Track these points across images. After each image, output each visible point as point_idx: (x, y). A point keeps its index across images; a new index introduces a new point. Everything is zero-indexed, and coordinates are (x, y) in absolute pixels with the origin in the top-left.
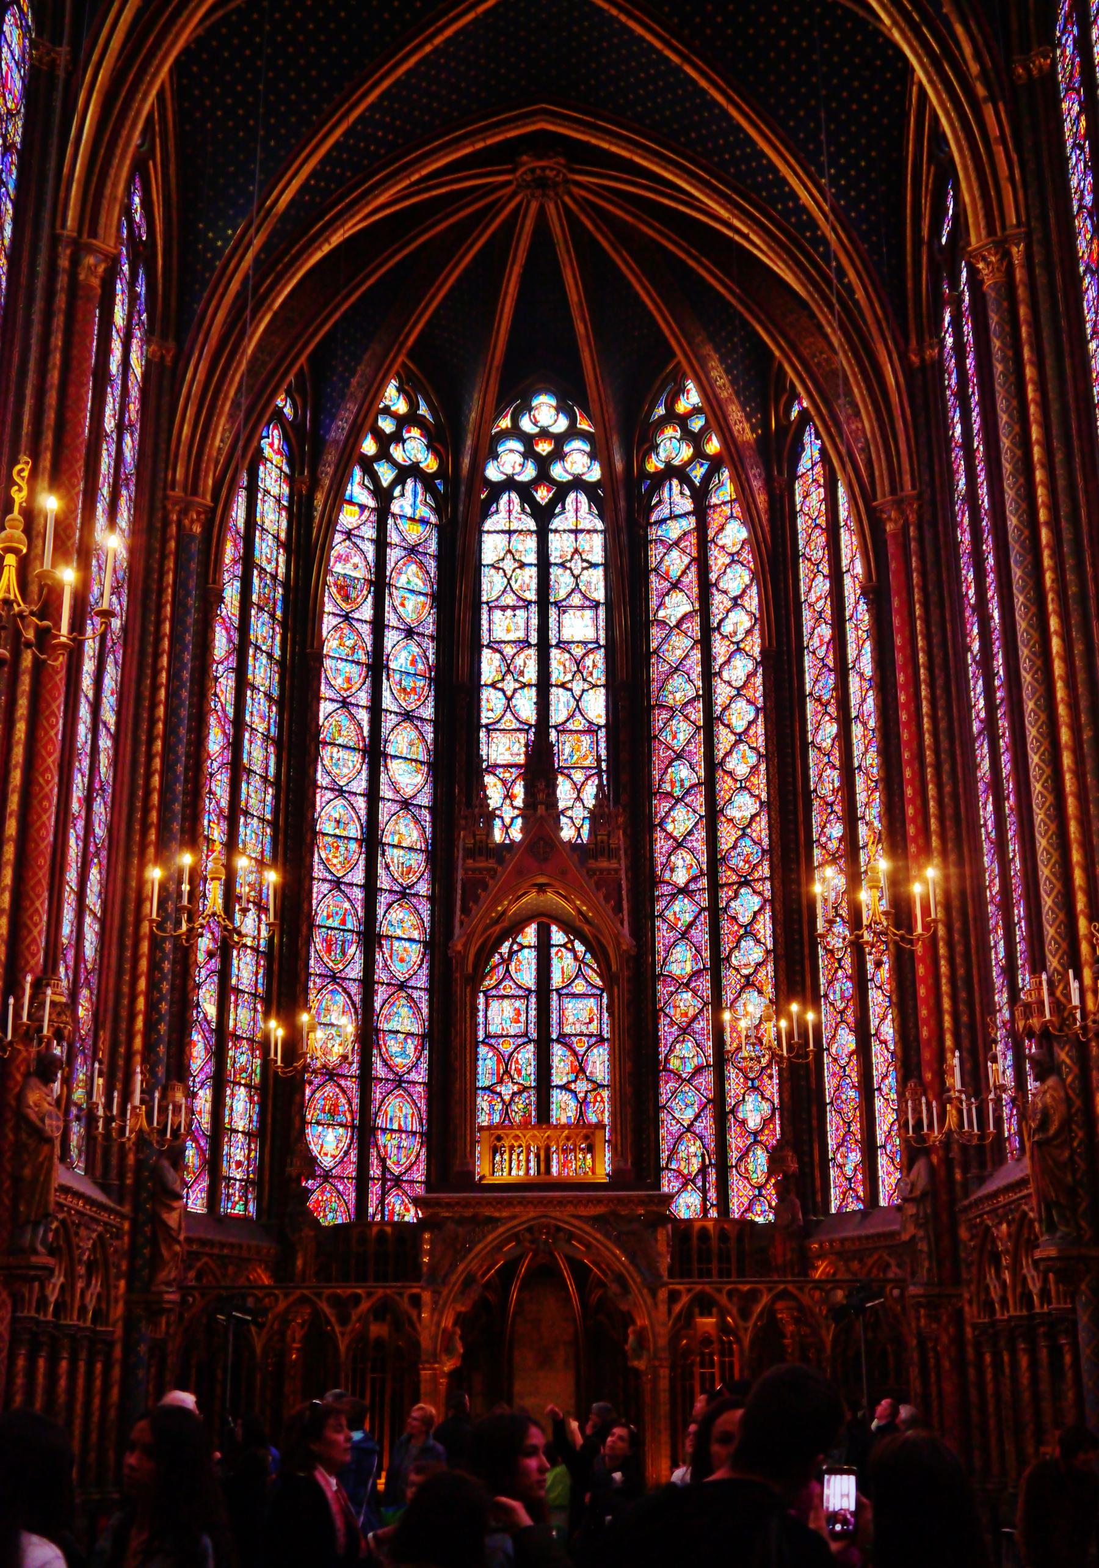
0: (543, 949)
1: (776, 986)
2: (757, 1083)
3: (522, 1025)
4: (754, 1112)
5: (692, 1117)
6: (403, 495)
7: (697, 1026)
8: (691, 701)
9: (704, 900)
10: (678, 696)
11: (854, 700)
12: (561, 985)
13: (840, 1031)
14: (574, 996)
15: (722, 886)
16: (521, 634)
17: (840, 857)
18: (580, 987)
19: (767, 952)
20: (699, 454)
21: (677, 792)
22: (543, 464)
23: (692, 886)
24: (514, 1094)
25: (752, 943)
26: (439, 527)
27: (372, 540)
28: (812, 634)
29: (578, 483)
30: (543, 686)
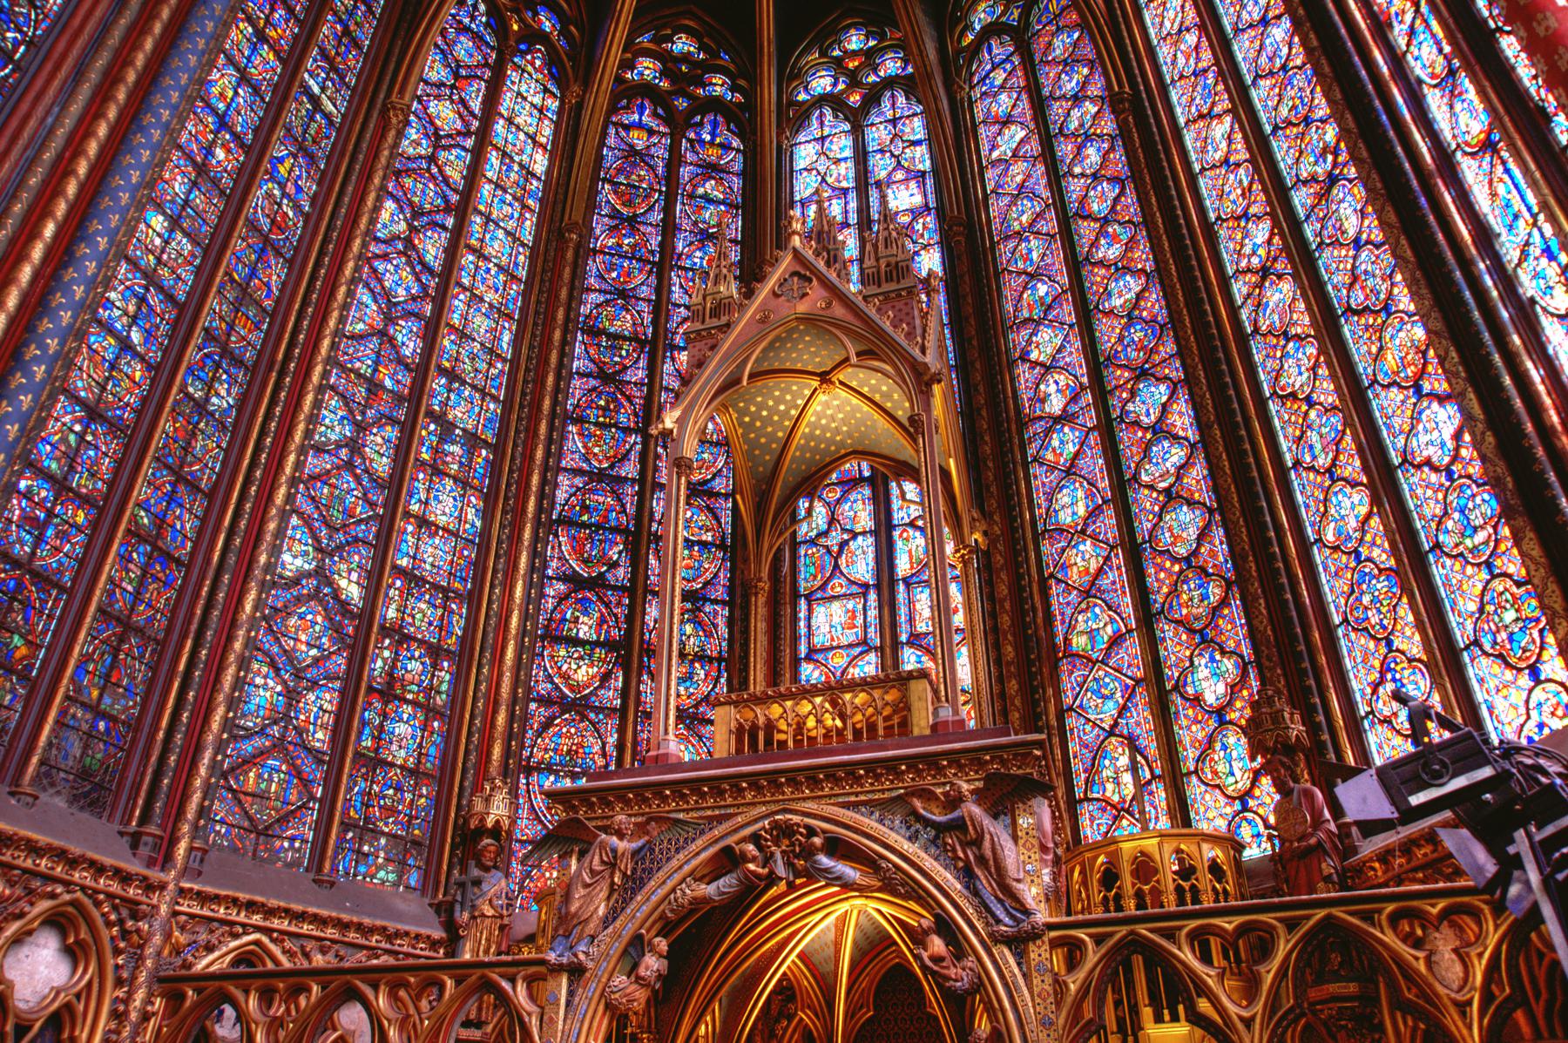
0: (884, 531)
1: (1216, 489)
2: (1211, 634)
3: (859, 630)
4: (1210, 683)
5: (1115, 713)
6: (701, 124)
7: (1105, 582)
8: (1039, 216)
10: (1024, 219)
11: (1244, 68)
12: (909, 572)
13: (1334, 499)
15: (1111, 392)
17: (1275, 259)
19: (1193, 446)
23: (1073, 408)
25: (1166, 444)
29: (890, 83)
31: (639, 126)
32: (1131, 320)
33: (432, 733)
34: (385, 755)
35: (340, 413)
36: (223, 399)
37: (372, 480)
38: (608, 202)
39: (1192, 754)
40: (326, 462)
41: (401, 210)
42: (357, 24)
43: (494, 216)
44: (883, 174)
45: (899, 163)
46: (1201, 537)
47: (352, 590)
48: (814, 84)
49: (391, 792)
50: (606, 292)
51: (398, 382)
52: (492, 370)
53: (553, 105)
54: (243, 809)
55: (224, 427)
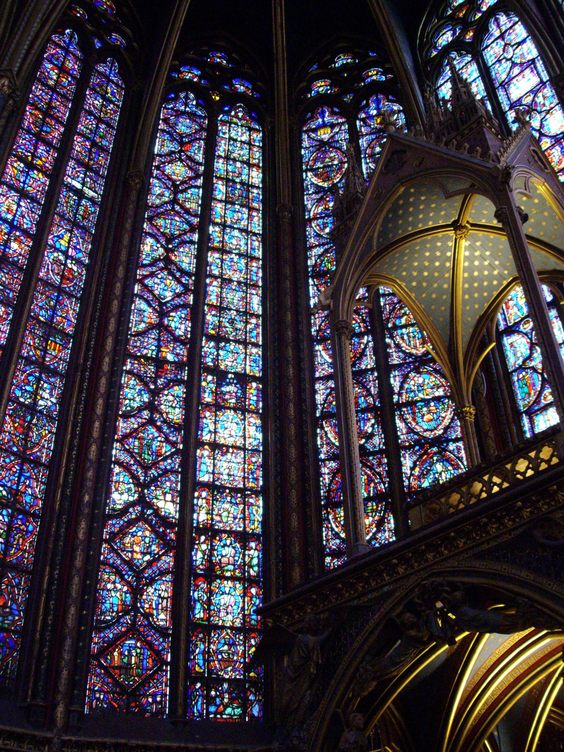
31: (324, 125)
33: (251, 598)
34: (215, 620)
35: (138, 388)
36: (48, 399)
37: (169, 427)
38: (312, 184)
40: (134, 423)
41: (158, 241)
42: (101, 137)
43: (229, 223)
44: (503, 77)
45: (513, 62)
47: (168, 507)
48: (440, 41)
49: (226, 648)
50: (324, 244)
51: (177, 355)
52: (249, 327)
53: (257, 137)
54: (114, 679)
55: (52, 418)
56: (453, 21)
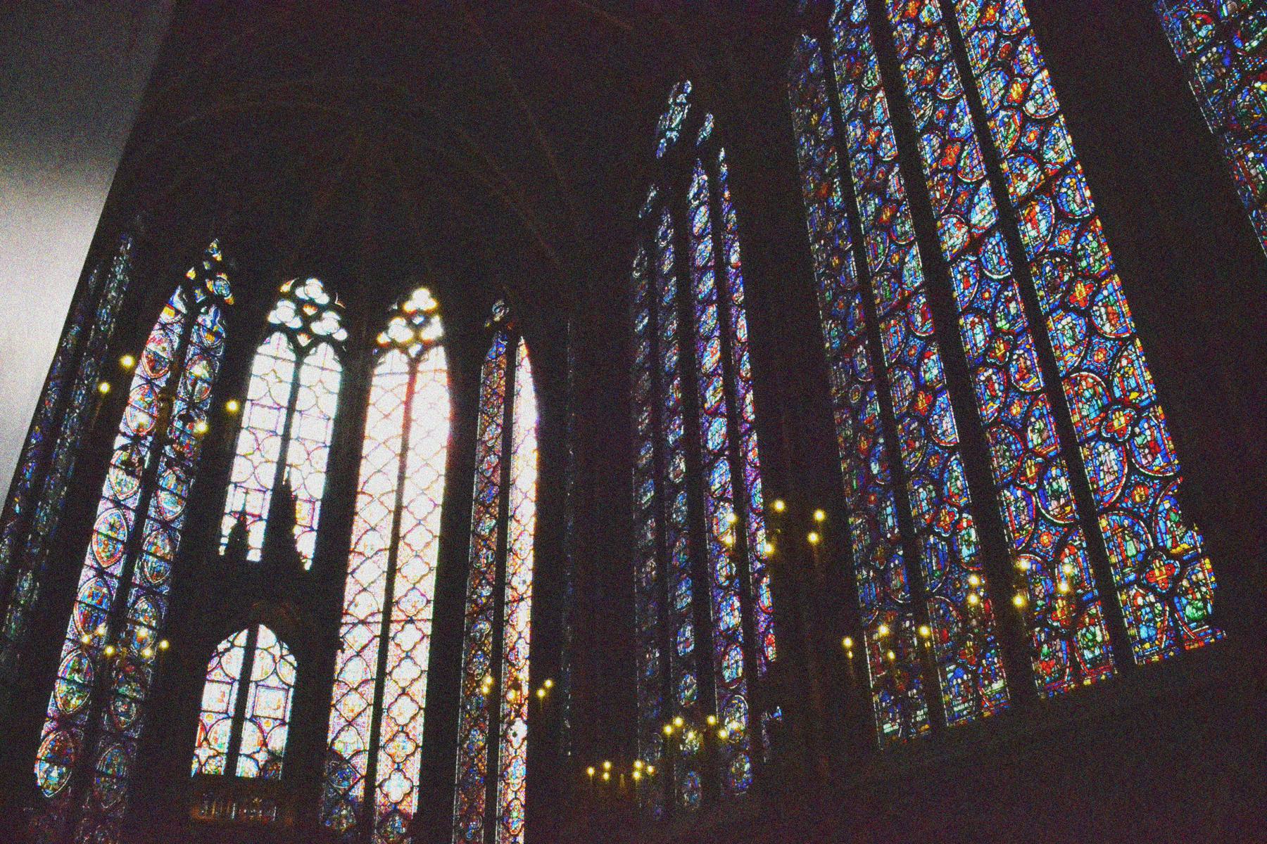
3: (225, 705)
6: (207, 312)
7: (360, 720)
9: (378, 630)
14: (268, 687)
16: (272, 427)
18: (273, 681)
20: (417, 339)
21: (368, 553)
22: (307, 320)
23: (370, 619)
24: (210, 757)
26: (227, 341)
27: (180, 336)
28: (482, 461)
29: (329, 339)
30: (282, 464)
32: (414, 588)
39: (377, 818)
46: (413, 718)
56: (300, 304)
